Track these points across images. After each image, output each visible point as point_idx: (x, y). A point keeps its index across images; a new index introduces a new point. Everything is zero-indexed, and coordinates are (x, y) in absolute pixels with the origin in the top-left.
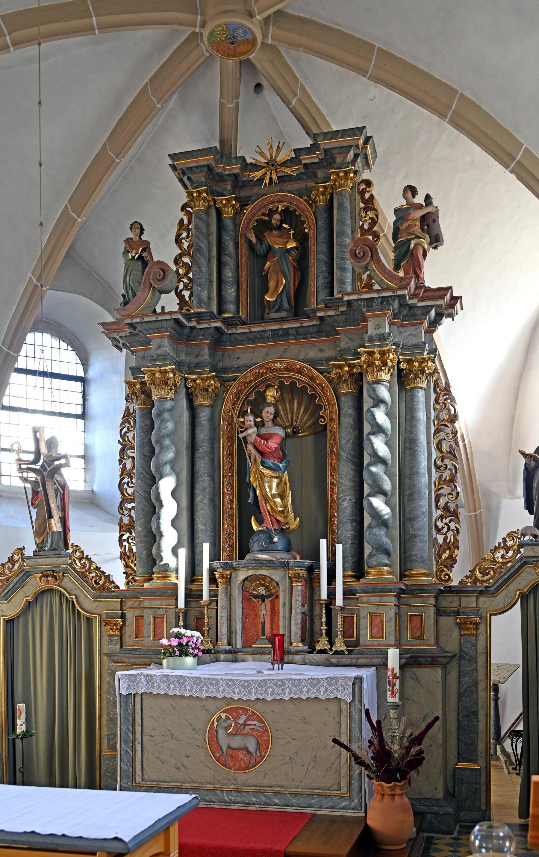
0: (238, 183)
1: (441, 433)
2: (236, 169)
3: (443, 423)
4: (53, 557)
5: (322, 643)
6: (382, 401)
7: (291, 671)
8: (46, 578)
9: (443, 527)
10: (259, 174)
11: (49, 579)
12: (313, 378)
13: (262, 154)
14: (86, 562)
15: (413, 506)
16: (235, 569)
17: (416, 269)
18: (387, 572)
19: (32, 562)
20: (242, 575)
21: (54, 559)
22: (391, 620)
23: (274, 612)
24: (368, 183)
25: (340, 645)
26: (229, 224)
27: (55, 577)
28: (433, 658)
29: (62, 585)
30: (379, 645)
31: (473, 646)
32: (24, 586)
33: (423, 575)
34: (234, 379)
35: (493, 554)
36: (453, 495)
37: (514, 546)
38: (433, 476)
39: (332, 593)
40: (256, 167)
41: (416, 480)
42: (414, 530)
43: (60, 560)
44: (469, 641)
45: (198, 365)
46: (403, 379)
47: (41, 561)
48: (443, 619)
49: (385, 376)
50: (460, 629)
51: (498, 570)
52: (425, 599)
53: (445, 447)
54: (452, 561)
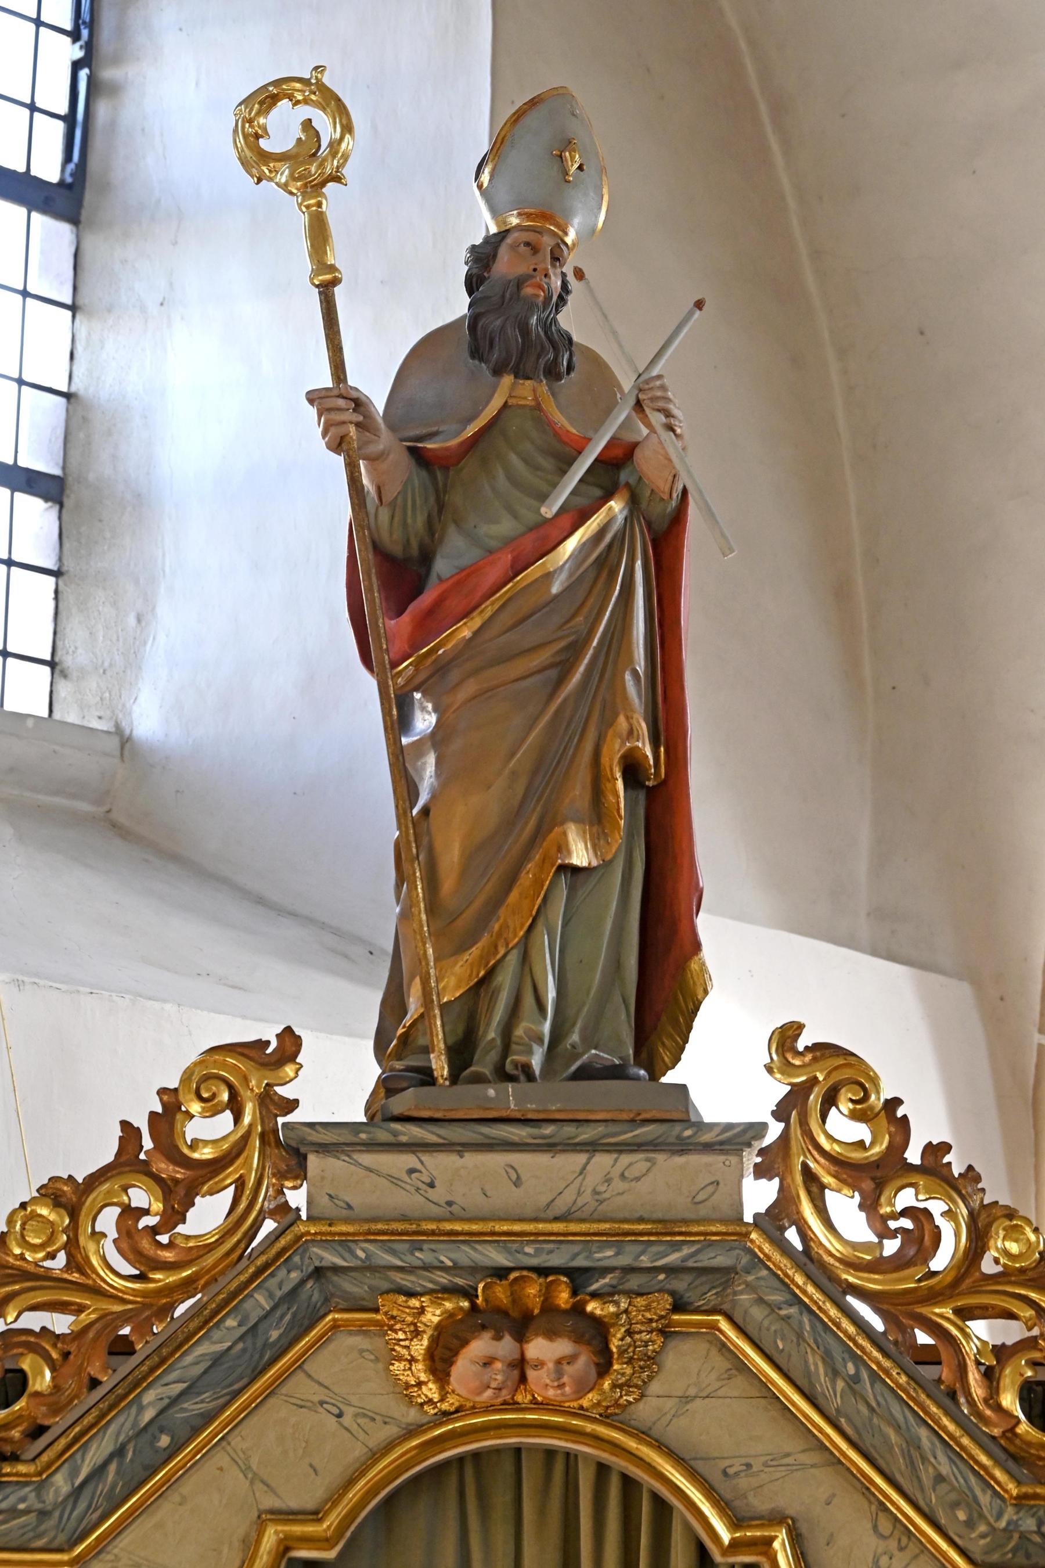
4: (592, 1147)
8: (506, 1346)
11: (538, 1348)
14: (937, 1207)
19: (378, 1183)
21: (603, 1161)
27: (595, 1334)
29: (644, 1412)
32: (250, 1410)
43: (660, 1183)
47: (471, 1179)
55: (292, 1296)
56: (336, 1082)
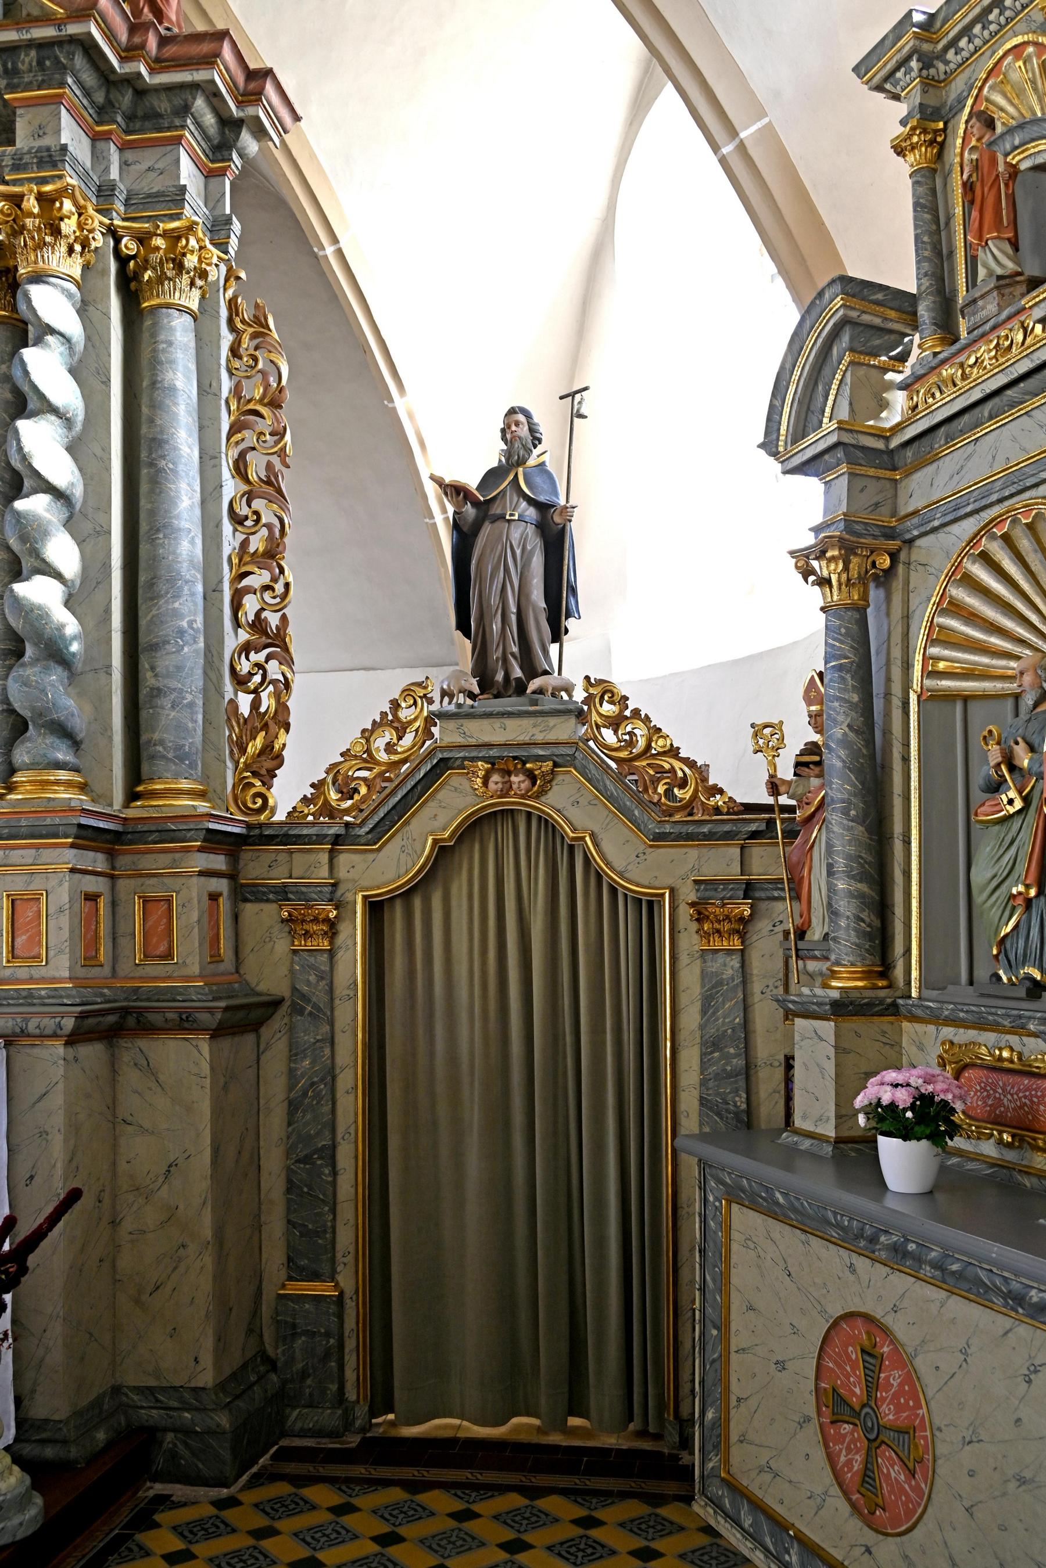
1: (246, 433)
3: (251, 406)
9: (251, 675)
15: (154, 612)
18: (69, 784)
22: (61, 911)
28: (181, 1013)
30: (31, 980)
31: (322, 978)
33: (179, 796)
35: (368, 741)
36: (273, 590)
37: (416, 719)
38: (225, 544)
41: (163, 545)
42: (156, 676)
44: (312, 967)
48: (249, 909)
50: (292, 934)
51: (378, 780)
52: (177, 856)
54: (270, 761)
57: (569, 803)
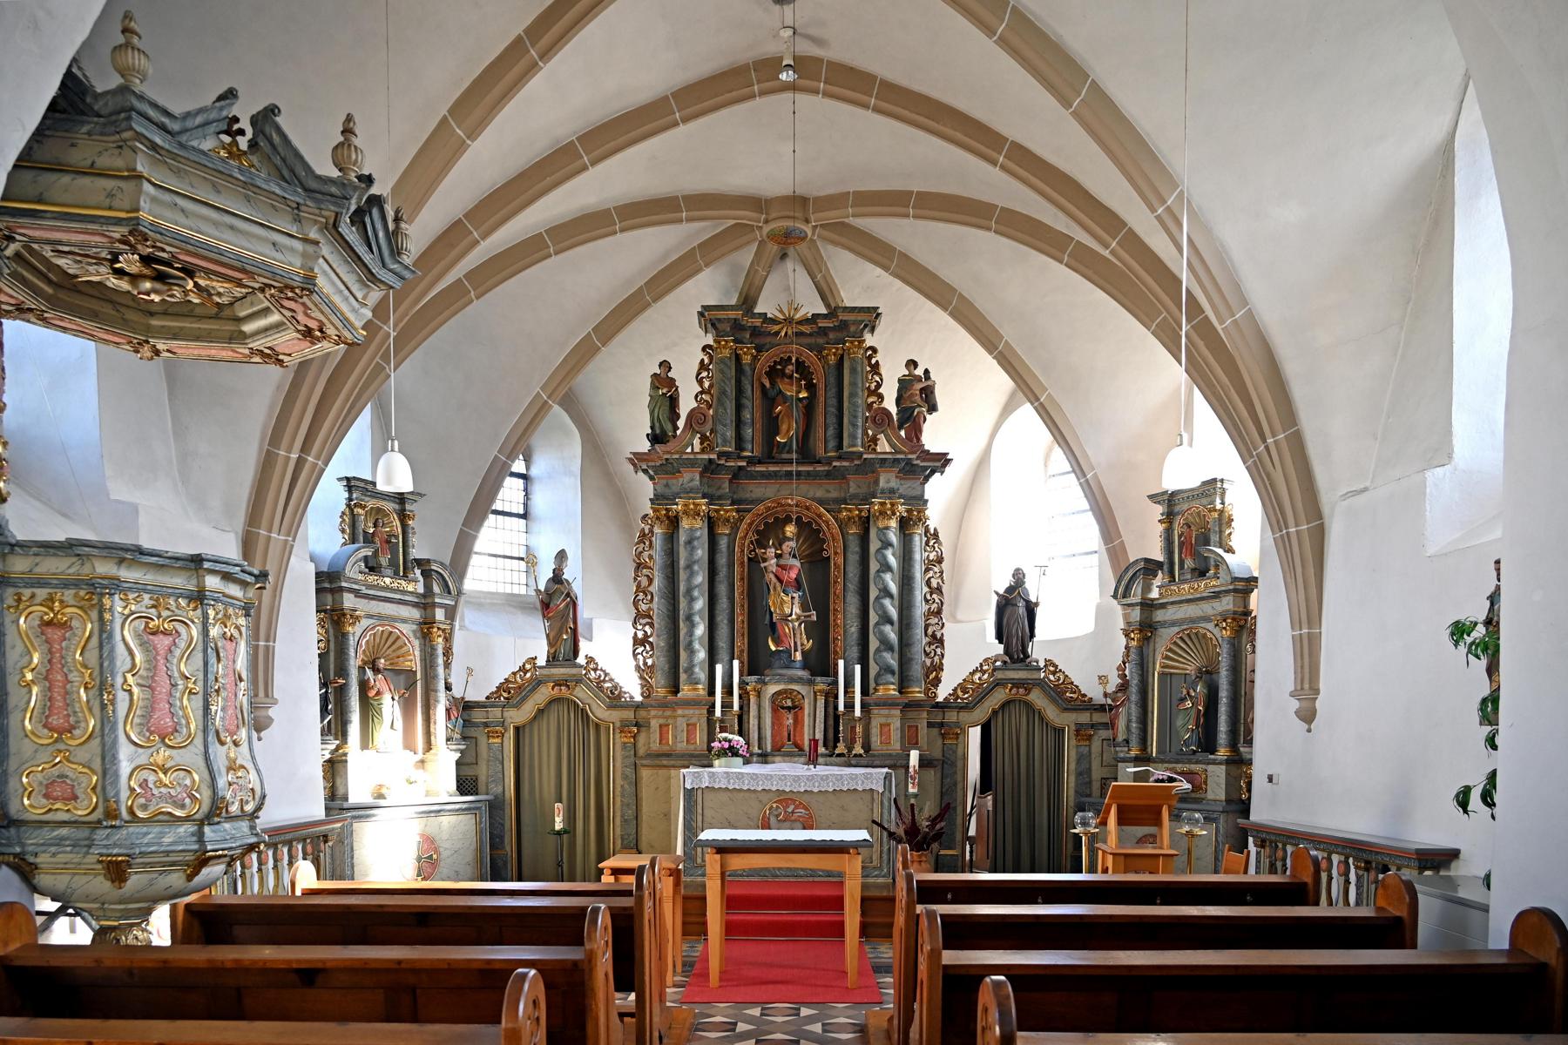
0: (755, 332)
2: (758, 322)
5: (841, 748)
6: (891, 545)
7: (821, 770)
10: (776, 328)
12: (820, 516)
13: (781, 311)
16: (765, 683)
17: (916, 431)
19: (545, 672)
20: (772, 689)
23: (798, 721)
24: (875, 350)
25: (858, 750)
26: (747, 369)
33: (917, 692)
34: (749, 511)
39: (850, 706)
40: (774, 321)
43: (574, 671)
45: (720, 498)
46: (905, 525)
47: (555, 671)
49: (893, 523)
53: (934, 583)
54: (937, 681)
55: (537, 683)
56: (542, 661)
57: (1036, 697)
